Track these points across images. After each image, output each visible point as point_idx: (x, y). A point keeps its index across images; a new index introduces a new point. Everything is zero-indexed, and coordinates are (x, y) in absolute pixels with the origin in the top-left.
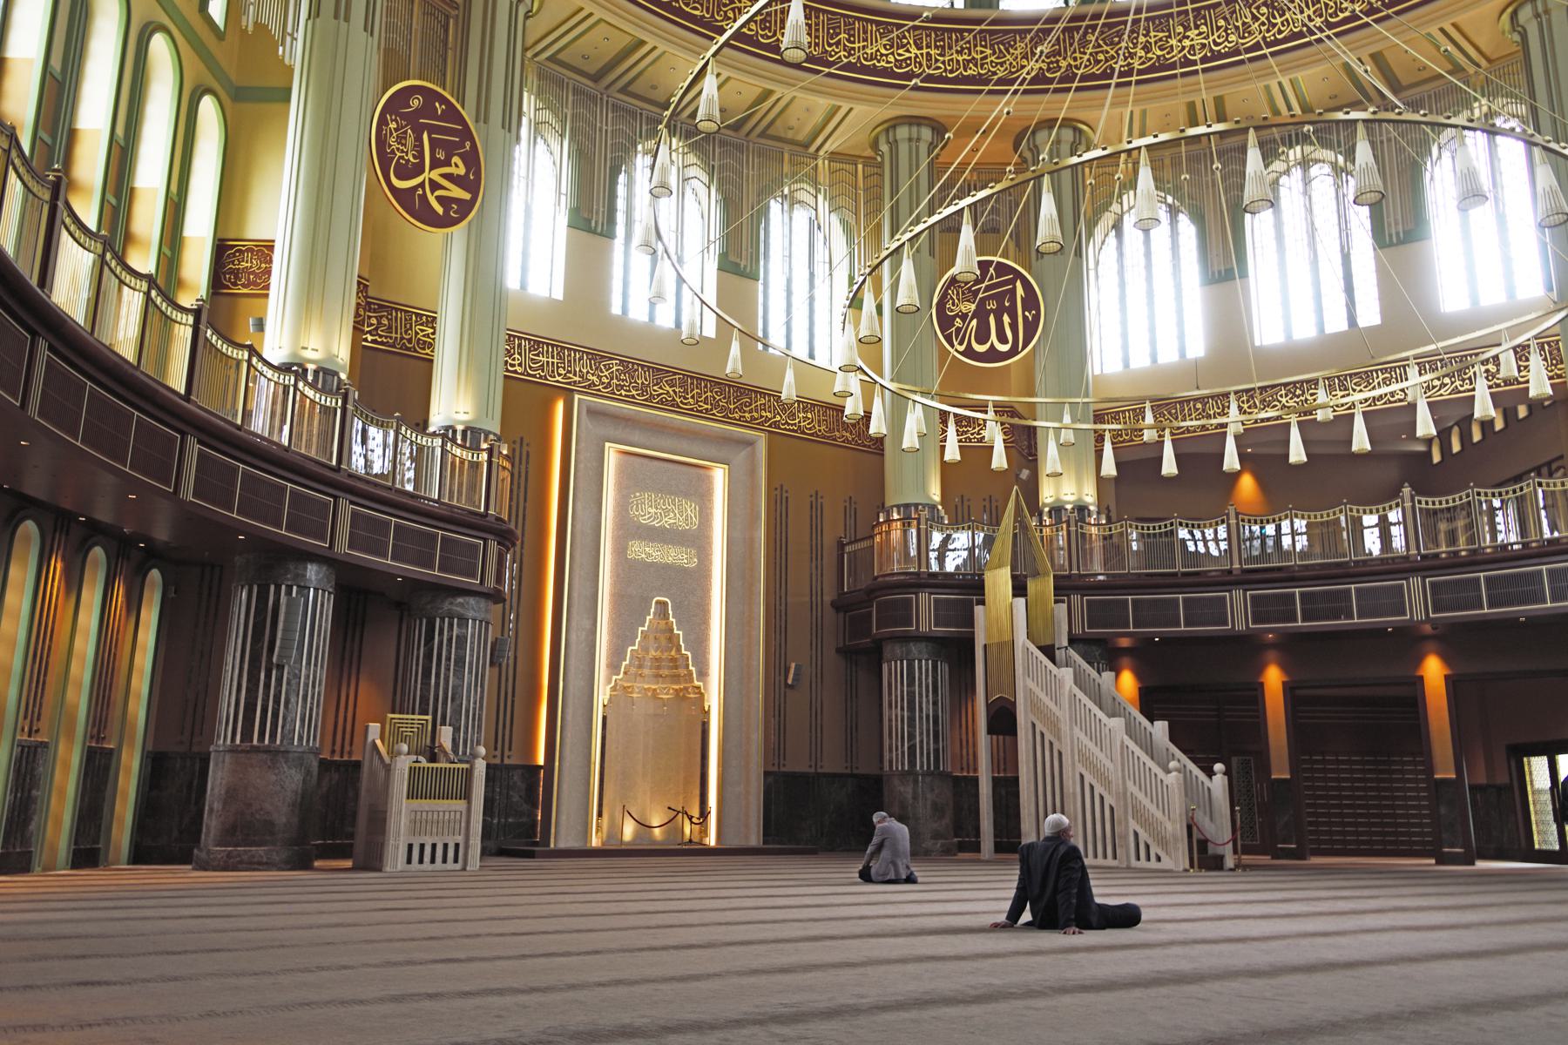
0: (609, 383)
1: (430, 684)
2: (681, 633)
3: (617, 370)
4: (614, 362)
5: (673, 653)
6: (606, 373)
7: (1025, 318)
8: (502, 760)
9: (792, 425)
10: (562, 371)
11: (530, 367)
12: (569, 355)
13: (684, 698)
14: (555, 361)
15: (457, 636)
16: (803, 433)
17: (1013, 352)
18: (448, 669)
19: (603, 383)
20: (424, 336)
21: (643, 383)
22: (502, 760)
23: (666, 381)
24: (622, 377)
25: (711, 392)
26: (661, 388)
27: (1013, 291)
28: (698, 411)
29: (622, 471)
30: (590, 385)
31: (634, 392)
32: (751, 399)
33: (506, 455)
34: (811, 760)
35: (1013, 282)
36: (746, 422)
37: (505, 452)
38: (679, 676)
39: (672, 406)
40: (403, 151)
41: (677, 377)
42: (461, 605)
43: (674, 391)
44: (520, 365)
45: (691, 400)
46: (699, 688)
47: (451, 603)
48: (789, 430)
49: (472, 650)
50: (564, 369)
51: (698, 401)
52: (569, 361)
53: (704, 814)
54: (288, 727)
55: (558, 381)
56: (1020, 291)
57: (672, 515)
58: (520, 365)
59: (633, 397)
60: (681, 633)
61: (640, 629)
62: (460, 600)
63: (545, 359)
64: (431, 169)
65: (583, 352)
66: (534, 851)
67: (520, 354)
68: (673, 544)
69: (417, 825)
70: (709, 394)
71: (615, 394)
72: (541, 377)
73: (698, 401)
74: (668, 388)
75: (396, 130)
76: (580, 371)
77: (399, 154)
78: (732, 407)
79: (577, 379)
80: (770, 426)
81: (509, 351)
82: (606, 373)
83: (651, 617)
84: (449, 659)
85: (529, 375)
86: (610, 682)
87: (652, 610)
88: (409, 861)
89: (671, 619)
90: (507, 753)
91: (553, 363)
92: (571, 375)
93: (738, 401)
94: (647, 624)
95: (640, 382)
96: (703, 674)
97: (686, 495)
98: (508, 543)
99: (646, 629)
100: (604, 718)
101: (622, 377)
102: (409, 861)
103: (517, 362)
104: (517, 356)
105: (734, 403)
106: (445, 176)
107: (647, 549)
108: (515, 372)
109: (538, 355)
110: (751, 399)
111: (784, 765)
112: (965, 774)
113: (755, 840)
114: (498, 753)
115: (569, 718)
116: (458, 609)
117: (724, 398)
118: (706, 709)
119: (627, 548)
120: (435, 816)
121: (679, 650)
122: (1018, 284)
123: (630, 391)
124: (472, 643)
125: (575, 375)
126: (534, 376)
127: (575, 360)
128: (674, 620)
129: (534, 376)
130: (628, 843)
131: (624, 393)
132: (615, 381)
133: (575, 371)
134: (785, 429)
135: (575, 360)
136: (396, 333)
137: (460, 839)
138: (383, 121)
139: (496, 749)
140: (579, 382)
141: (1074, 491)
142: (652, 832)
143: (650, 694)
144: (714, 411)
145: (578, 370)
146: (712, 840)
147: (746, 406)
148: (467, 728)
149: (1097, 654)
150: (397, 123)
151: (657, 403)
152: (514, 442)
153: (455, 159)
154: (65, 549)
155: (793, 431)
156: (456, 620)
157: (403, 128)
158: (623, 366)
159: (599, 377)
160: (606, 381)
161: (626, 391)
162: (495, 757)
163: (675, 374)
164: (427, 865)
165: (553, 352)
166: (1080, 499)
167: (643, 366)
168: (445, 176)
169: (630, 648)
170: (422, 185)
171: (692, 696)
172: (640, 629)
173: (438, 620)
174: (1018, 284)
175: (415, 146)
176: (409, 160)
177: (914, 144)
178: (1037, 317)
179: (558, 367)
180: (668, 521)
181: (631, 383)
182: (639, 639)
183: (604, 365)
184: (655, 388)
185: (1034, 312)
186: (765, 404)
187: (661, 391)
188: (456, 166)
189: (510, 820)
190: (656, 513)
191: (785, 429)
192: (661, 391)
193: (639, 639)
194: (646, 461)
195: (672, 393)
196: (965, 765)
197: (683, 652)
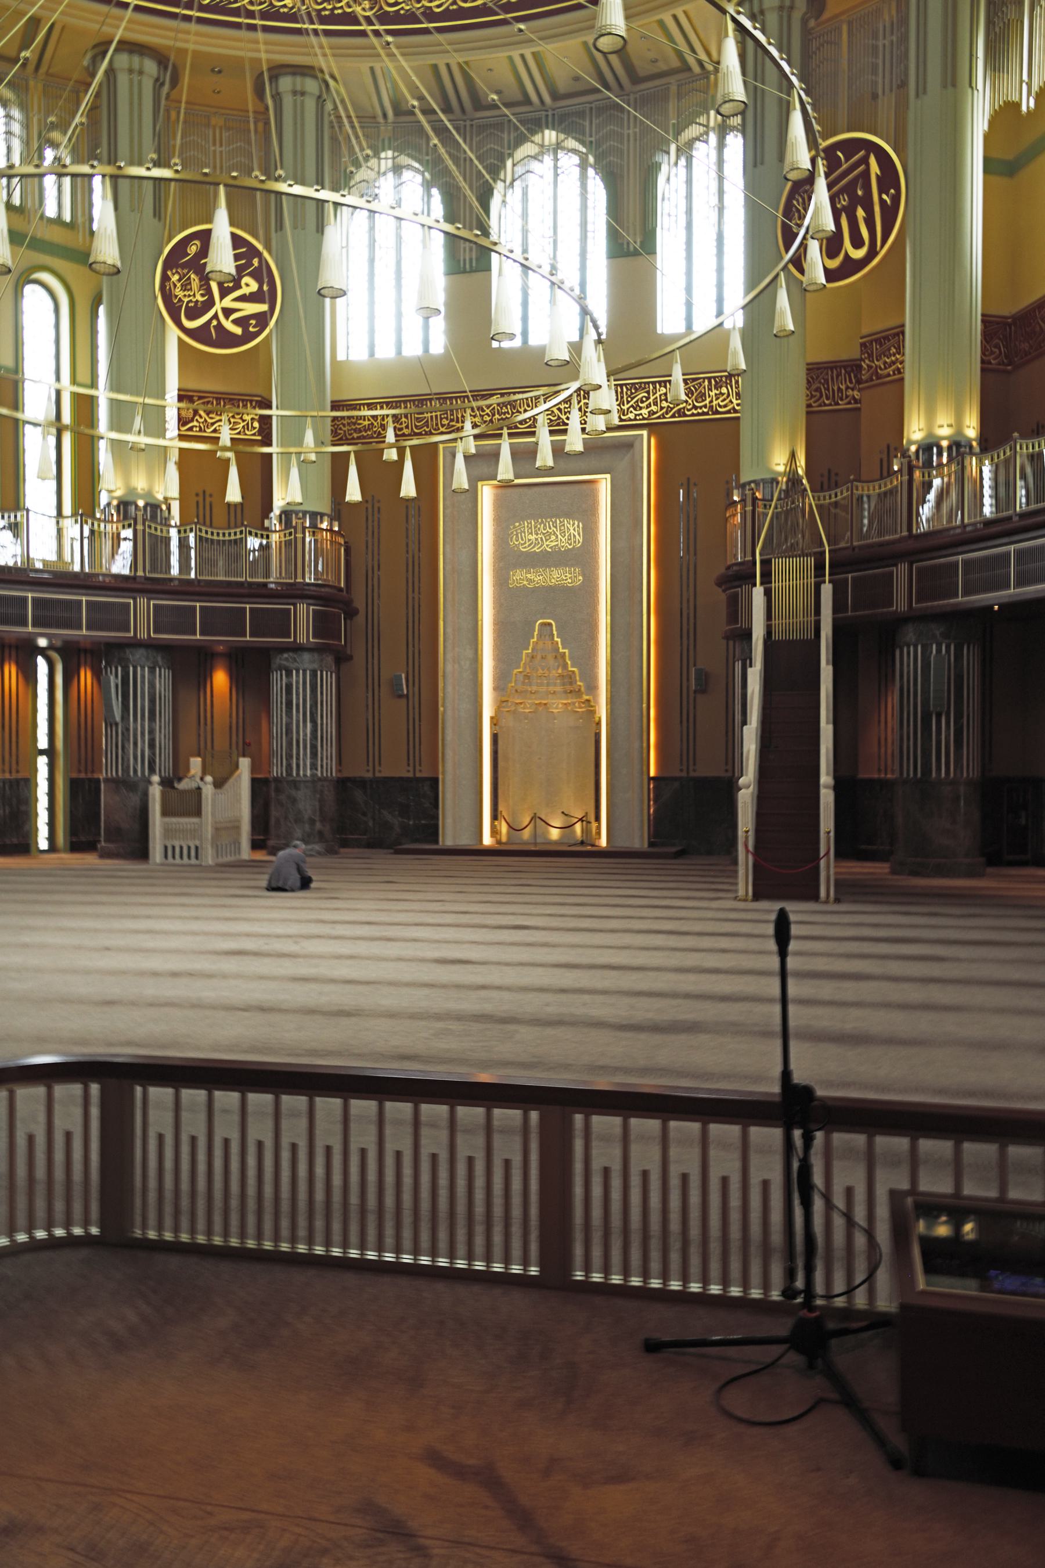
0: (491, 421)
2: (566, 651)
5: (560, 671)
6: (488, 411)
7: (882, 202)
9: (701, 408)
10: (445, 422)
11: (416, 427)
15: (286, 685)
16: (717, 412)
17: (872, 253)
18: (281, 711)
24: (504, 410)
27: (867, 173)
29: (500, 505)
32: (648, 392)
34: (727, 764)
35: (865, 160)
36: (644, 419)
39: (558, 425)
40: (189, 296)
42: (286, 659)
44: (407, 427)
47: (280, 659)
48: (699, 414)
50: (447, 418)
53: (598, 818)
54: (125, 764)
56: (875, 168)
57: (553, 537)
58: (407, 427)
62: (286, 655)
64: (222, 298)
68: (556, 567)
69: (168, 832)
75: (179, 280)
77: (186, 300)
78: (625, 407)
80: (673, 416)
82: (488, 411)
83: (535, 640)
88: (166, 857)
89: (556, 639)
90: (418, 768)
92: (454, 423)
93: (632, 399)
94: (530, 648)
96: (592, 688)
97: (569, 515)
99: (530, 651)
101: (504, 410)
102: (166, 857)
103: (404, 425)
104: (404, 419)
105: (628, 402)
106: (242, 299)
107: (529, 576)
110: (648, 392)
111: (694, 770)
112: (883, 776)
113: (638, 841)
114: (411, 769)
119: (508, 578)
121: (565, 666)
122: (873, 161)
124: (298, 688)
128: (559, 640)
130: (556, 843)
132: (497, 416)
133: (457, 418)
134: (693, 415)
138: (165, 278)
141: (952, 421)
142: (548, 832)
145: (460, 416)
146: (603, 842)
147: (642, 402)
148: (298, 754)
149: (938, 633)
150: (179, 273)
153: (246, 280)
154: (17, 656)
155: (704, 414)
157: (185, 276)
160: (488, 419)
164: (178, 861)
166: (930, 435)
168: (242, 299)
170: (216, 316)
172: (525, 652)
174: (873, 161)
175: (201, 286)
176: (197, 301)
177: (785, 14)
178: (896, 199)
179: (441, 419)
180: (548, 545)
181: (513, 413)
185: (892, 191)
186: (665, 394)
188: (247, 285)
189: (423, 822)
190: (536, 539)
191: (693, 415)
194: (525, 490)
195: (556, 412)
196: (883, 767)
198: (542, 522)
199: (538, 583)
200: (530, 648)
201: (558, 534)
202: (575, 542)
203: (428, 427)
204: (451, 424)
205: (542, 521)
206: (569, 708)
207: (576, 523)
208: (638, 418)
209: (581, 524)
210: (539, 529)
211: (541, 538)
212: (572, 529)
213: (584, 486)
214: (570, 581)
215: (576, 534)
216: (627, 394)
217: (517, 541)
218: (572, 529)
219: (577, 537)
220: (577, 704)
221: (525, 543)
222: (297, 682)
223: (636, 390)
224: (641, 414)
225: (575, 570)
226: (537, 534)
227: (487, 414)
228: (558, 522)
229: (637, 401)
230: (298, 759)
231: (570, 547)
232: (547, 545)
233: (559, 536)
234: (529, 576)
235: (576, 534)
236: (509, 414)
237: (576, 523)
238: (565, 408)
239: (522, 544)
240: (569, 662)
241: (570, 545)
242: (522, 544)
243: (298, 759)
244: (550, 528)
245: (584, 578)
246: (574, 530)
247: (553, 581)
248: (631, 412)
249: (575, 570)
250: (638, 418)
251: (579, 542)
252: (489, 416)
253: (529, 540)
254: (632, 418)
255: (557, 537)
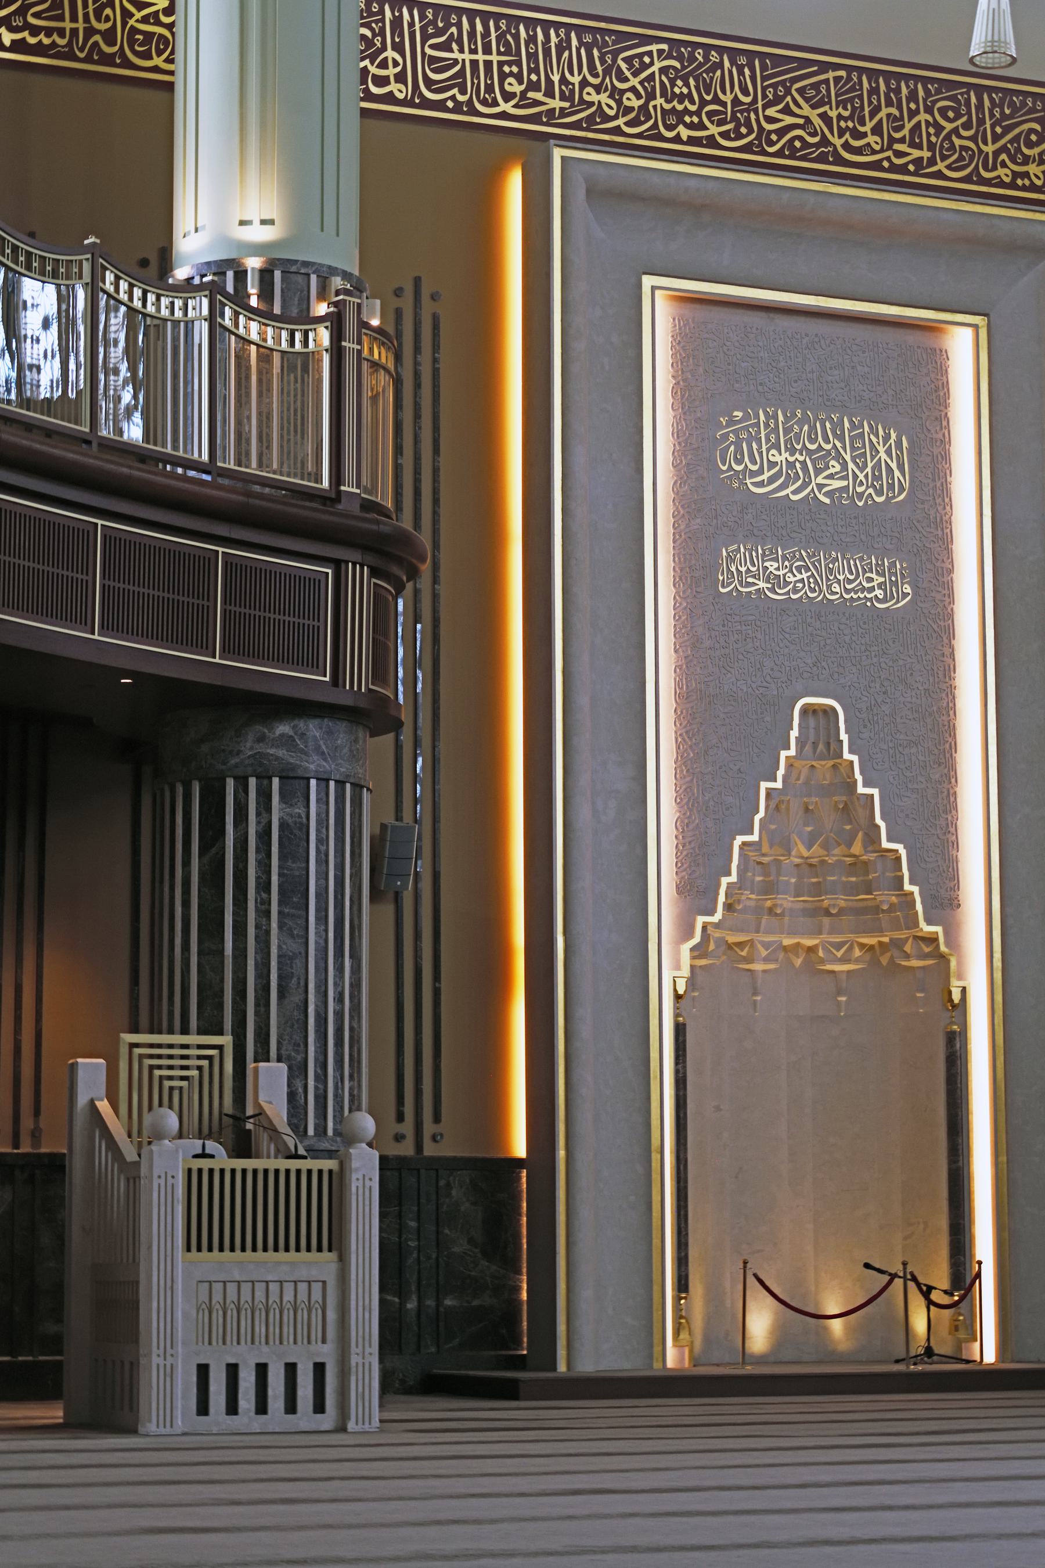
0: (644, 108)
1: (222, 951)
2: (875, 792)
3: (663, 70)
4: (654, 48)
5: (857, 848)
6: (634, 82)
8: (419, 1146)
10: (514, 86)
11: (429, 83)
12: (532, 39)
13: (894, 968)
14: (495, 58)
15: (283, 826)
18: (264, 913)
19: (631, 109)
20: (145, 20)
21: (736, 101)
22: (419, 1146)
23: (801, 91)
25: (929, 110)
26: (787, 111)
28: (894, 169)
30: (590, 119)
31: (714, 130)
33: (379, 330)
36: (1033, 188)
37: (375, 322)
38: (877, 909)
39: (822, 159)
41: (831, 75)
42: (287, 742)
43: (824, 116)
44: (401, 78)
45: (871, 139)
46: (933, 940)
47: (261, 739)
49: (323, 860)
51: (892, 141)
52: (532, 57)
55: (504, 116)
57: (835, 467)
58: (401, 78)
59: (711, 142)
60: (875, 792)
61: (764, 785)
62: (283, 729)
63: (467, 56)
65: (569, 27)
66: (515, 1382)
67: (399, 48)
68: (844, 549)
70: (923, 117)
71: (660, 138)
72: (458, 108)
73: (892, 141)
74: (806, 110)
76: (563, 80)
78: (990, 149)
79: (556, 104)
81: (368, 42)
82: (634, 82)
83: (792, 752)
84: (264, 886)
85: (427, 104)
86: (689, 934)
87: (794, 733)
89: (847, 755)
91: (488, 64)
92: (539, 96)
93: (1007, 130)
94: (781, 773)
95: (728, 98)
98: (396, 570)
99: (779, 784)
100: (680, 1030)
103: (391, 71)
104: (390, 54)
105: (996, 138)
107: (772, 566)
108: (390, 98)
109: (446, 47)
114: (407, 1127)
115: (585, 1031)
116: (281, 753)
117: (967, 126)
118: (956, 997)
119: (716, 567)
120: (260, 1295)
123: (702, 127)
124: (322, 841)
125: (550, 94)
126: (440, 106)
127: (547, 52)
129: (440, 106)
130: (761, 1359)
131: (685, 133)
132: (659, 101)
133: (550, 82)
135: (547, 52)
136: (74, 19)
137: (327, 1353)
139: (400, 1118)
140: (563, 113)
142: (826, 1329)
143: (798, 962)
144: (941, 166)
145: (556, 78)
147: (1030, 145)
151: (779, 154)
152: (398, 292)
156: (276, 781)
158: (680, 58)
159: (617, 94)
160: (636, 103)
161: (691, 126)
162: (399, 1138)
163: (825, 67)
165: (486, 34)
167: (733, 53)
169: (739, 840)
171: (915, 963)
172: (764, 785)
173: (230, 783)
181: (703, 103)
182: (762, 813)
183: (628, 60)
184: (771, 112)
187: (789, 120)
189: (448, 1302)
190: (791, 465)
192: (789, 120)
193: (762, 813)
194: (757, 319)
195: (817, 122)
197: (885, 844)
198: (805, 419)
199: (795, 591)
200: (781, 773)
201: (848, 458)
202: (891, 487)
203: (463, 92)
204: (530, 95)
205: (804, 414)
206: (884, 960)
207: (893, 436)
208: (1019, 182)
209: (905, 444)
210: (798, 436)
211: (804, 463)
212: (881, 449)
213: (912, 338)
214: (879, 593)
215: (894, 465)
216: (992, 116)
217: (739, 462)
218: (881, 449)
219: (897, 473)
220: (908, 948)
221: (761, 471)
222: (323, 822)
223: (1015, 110)
224: (1026, 175)
225: (893, 565)
226: (792, 451)
227: (633, 89)
228: (847, 425)
229: (1016, 139)
230: (322, 1078)
231: (879, 500)
232: (821, 486)
233: (851, 465)
234: (772, 566)
235: (894, 465)
236: (693, 102)
237: (893, 436)
238: (840, 117)
239: (753, 474)
240: (882, 825)
241: (880, 493)
242: (753, 474)
243: (322, 1078)
244: (827, 440)
245: (915, 587)
246: (888, 452)
247: (836, 588)
248: (1004, 165)
249: (893, 565)
250: (1019, 182)
251: (902, 489)
252: (639, 96)
253: (772, 465)
254: (1007, 180)
255: (844, 466)
